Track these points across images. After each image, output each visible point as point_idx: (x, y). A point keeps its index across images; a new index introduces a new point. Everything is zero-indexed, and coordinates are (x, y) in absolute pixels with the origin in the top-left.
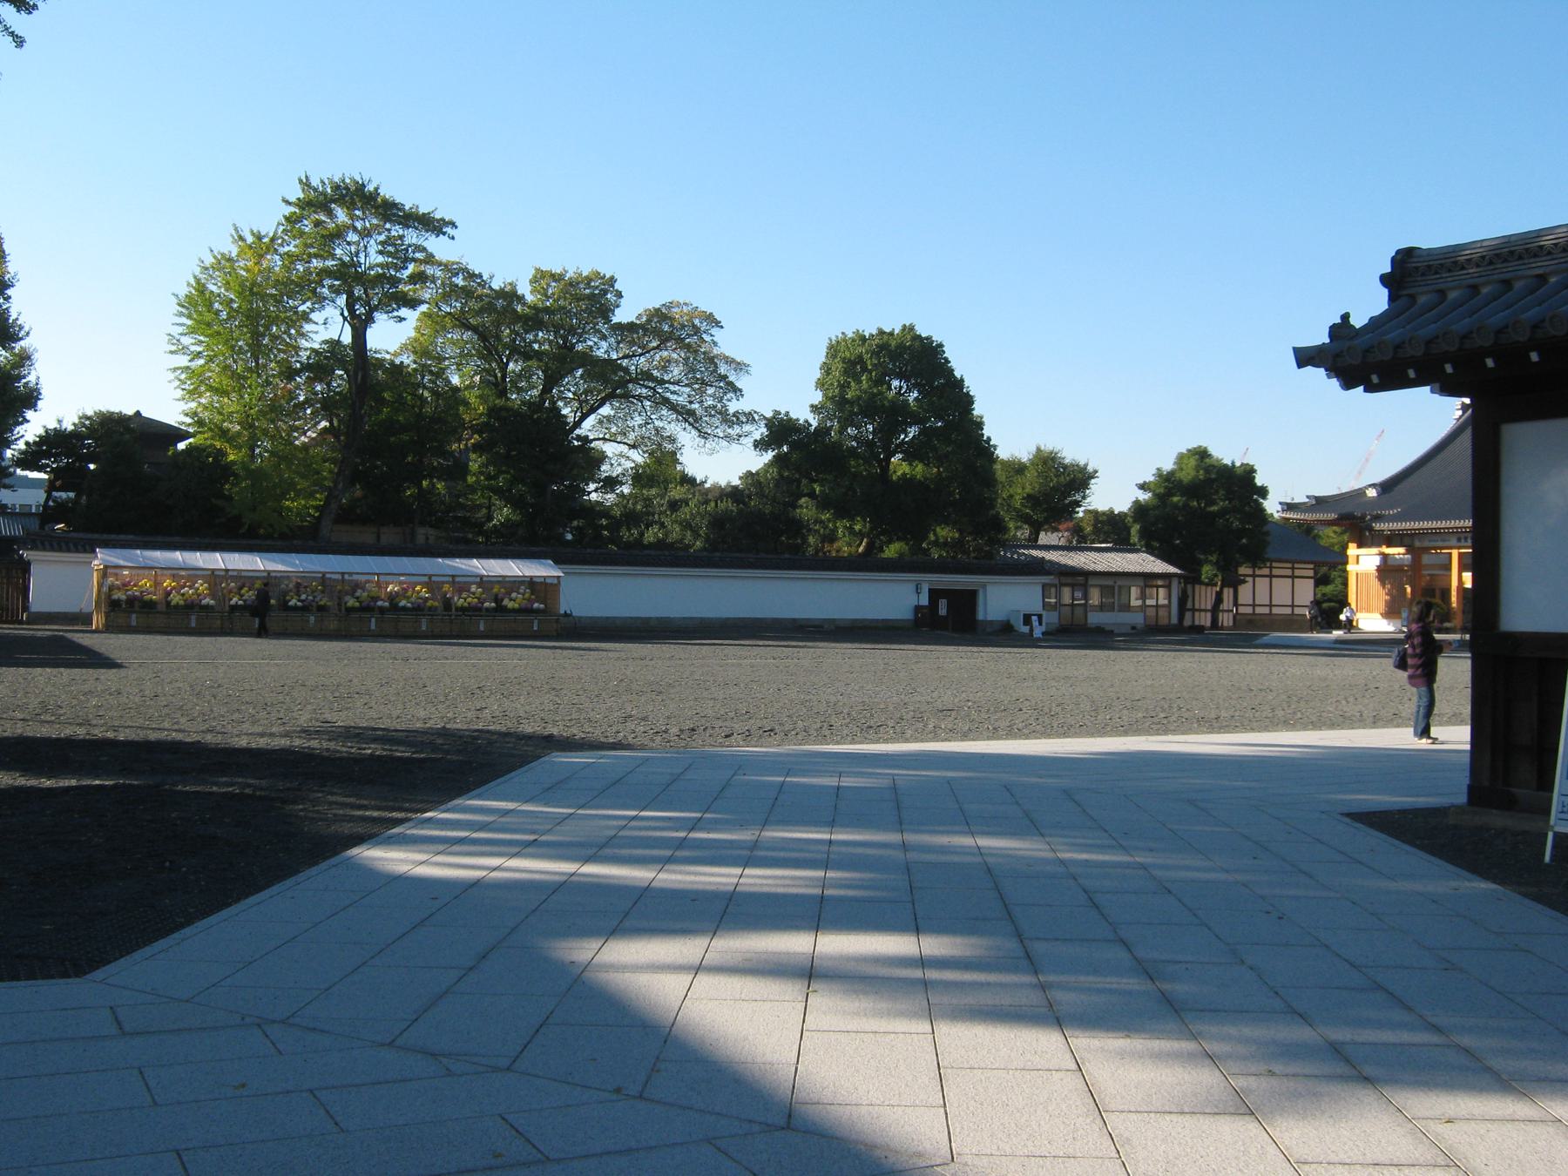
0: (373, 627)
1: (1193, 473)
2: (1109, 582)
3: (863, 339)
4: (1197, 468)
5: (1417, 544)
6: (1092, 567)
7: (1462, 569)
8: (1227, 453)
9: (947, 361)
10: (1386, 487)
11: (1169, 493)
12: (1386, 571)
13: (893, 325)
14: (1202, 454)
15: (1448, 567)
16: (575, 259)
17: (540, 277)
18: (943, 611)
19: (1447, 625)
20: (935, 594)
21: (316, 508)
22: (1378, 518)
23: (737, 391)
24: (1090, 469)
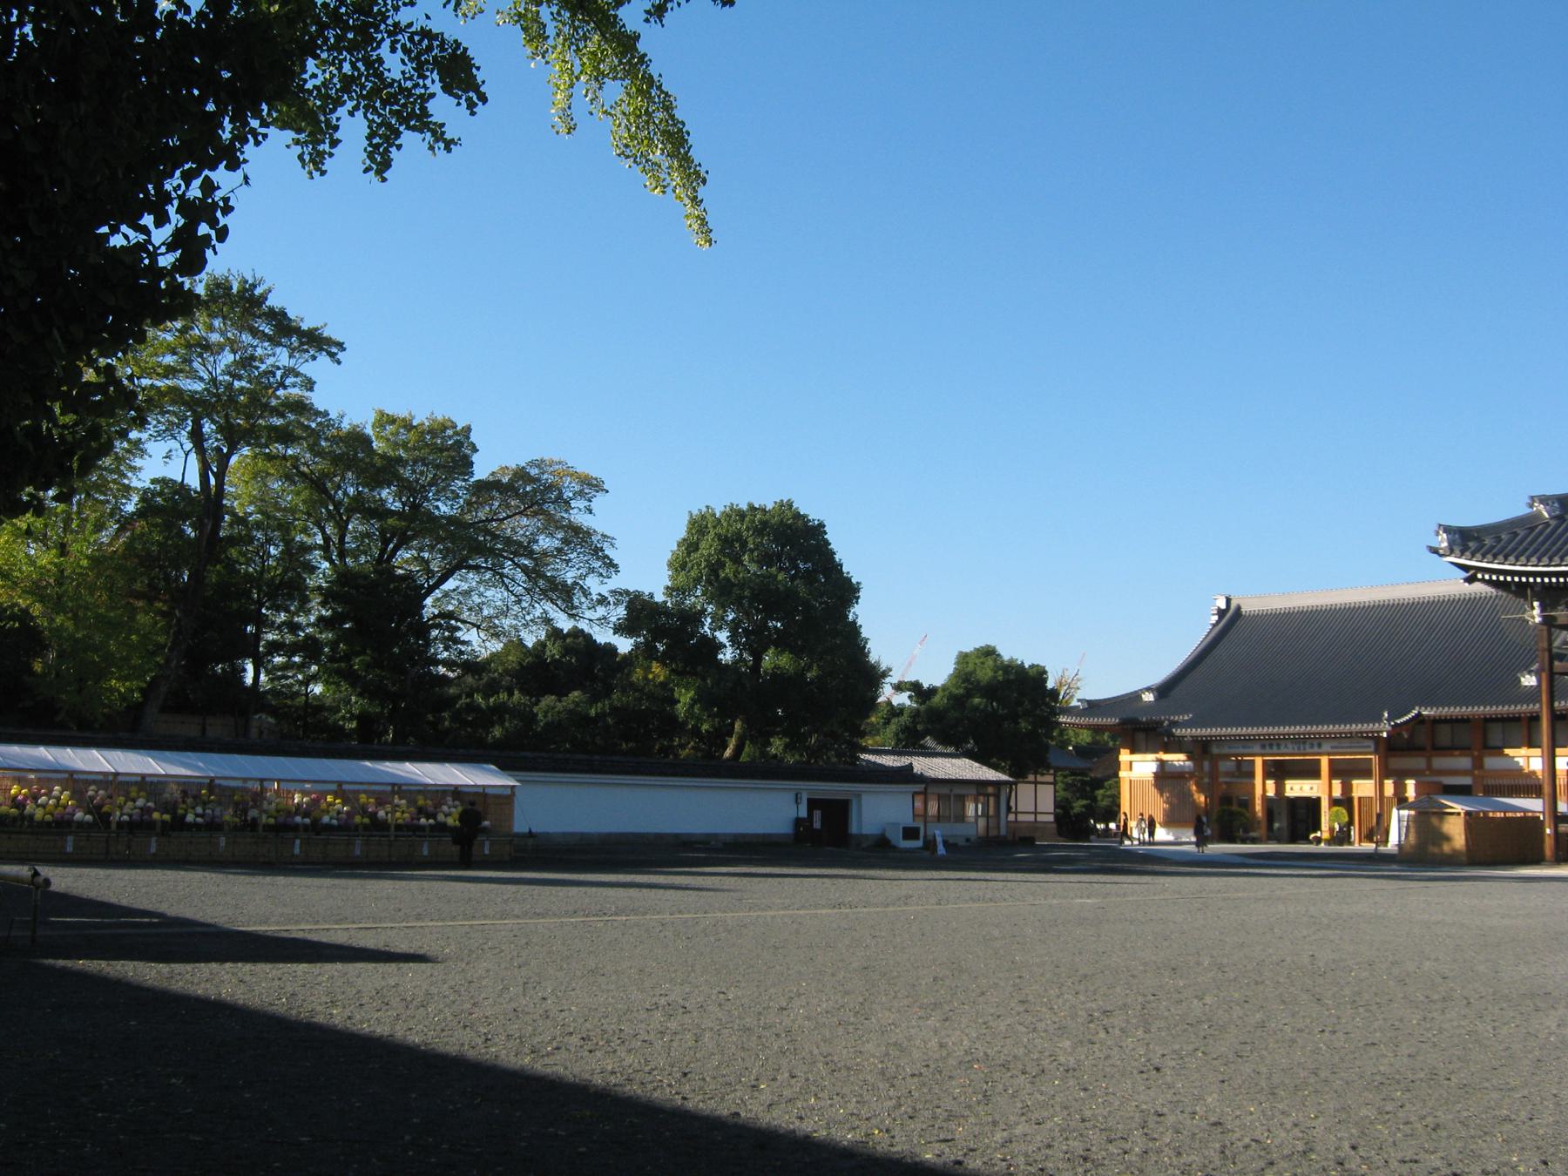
0: (297, 851)
1: (990, 674)
2: (945, 790)
3: (741, 515)
4: (996, 669)
5: (1215, 750)
6: (931, 774)
7: (1267, 775)
8: (1018, 650)
9: (827, 543)
10: (1163, 690)
11: (969, 694)
12: (1164, 777)
13: (767, 499)
14: (989, 652)
15: (1252, 775)
16: (422, 405)
17: (384, 420)
18: (817, 825)
19: (1253, 834)
20: (813, 804)
21: (141, 690)
22: (1175, 724)
23: (611, 565)
24: (883, 667)
